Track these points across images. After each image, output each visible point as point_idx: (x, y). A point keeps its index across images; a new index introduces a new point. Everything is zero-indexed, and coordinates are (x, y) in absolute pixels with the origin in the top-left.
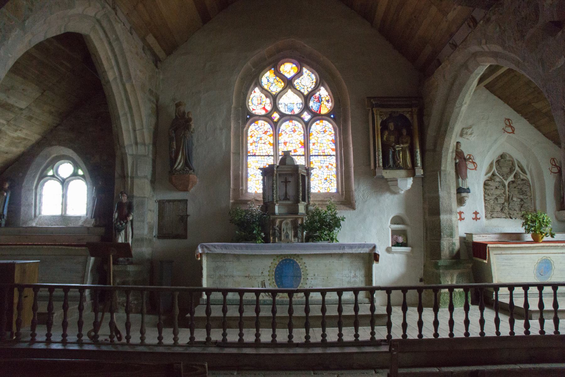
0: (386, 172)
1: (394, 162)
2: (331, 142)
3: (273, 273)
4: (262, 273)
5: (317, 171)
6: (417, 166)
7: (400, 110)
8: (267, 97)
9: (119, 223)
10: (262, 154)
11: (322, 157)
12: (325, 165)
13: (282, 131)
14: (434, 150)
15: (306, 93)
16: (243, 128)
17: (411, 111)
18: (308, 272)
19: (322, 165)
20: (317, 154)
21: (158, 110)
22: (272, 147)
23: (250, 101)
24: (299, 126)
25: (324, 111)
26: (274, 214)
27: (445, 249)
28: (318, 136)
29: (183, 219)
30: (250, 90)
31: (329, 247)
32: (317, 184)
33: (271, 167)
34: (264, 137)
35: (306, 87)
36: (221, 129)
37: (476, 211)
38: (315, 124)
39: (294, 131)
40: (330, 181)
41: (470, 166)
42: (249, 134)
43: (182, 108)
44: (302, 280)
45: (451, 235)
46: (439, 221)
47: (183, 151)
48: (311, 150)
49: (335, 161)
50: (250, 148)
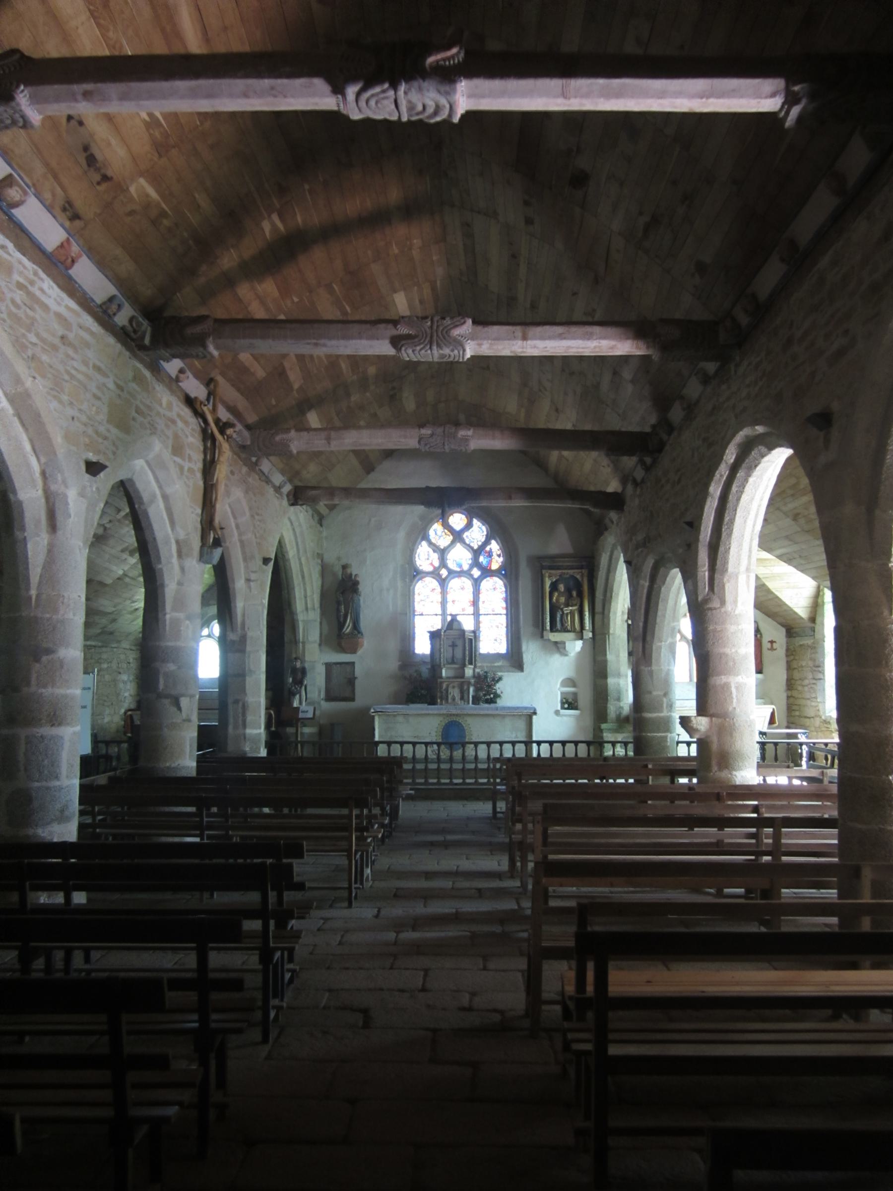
1: (562, 625)
6: (585, 630)
7: (571, 572)
8: (434, 551)
9: (293, 688)
14: (603, 613)
15: (476, 547)
16: (410, 586)
17: (581, 572)
21: (325, 569)
23: (417, 556)
24: (468, 583)
25: (495, 566)
26: (441, 677)
27: (612, 712)
29: (351, 681)
30: (417, 544)
31: (488, 709)
33: (439, 631)
35: (475, 541)
36: (388, 590)
43: (349, 571)
45: (619, 699)
46: (606, 685)
47: (351, 613)
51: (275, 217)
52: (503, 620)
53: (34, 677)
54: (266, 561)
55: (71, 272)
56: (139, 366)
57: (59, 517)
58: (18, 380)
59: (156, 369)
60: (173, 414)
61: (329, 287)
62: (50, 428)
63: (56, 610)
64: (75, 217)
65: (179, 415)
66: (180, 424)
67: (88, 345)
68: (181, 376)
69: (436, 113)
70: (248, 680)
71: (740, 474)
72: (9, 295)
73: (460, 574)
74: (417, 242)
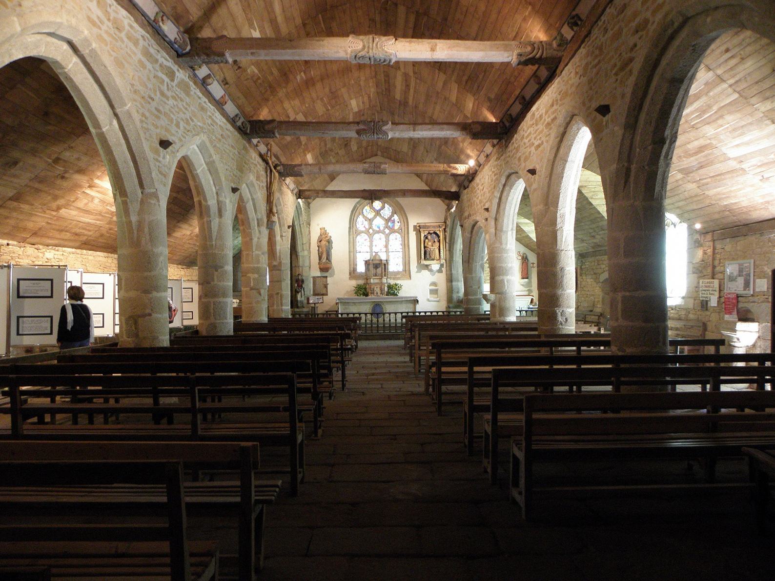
33: (369, 260)
45: (458, 292)
51: (302, 74)
52: (401, 254)
53: (215, 277)
54: (289, 227)
55: (224, 107)
56: (245, 142)
57: (223, 211)
58: (211, 156)
59: (249, 142)
60: (255, 162)
61: (322, 99)
62: (221, 175)
63: (223, 250)
64: (227, 83)
65: (258, 162)
66: (258, 166)
67: (229, 137)
68: (259, 144)
69: (384, 62)
70: (283, 283)
71: (507, 188)
72: (207, 121)
73: (378, 232)
74: (363, 78)
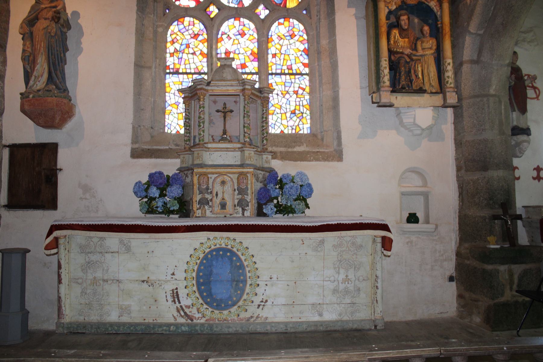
0: (396, 98)
2: (303, 54)
3: (194, 275)
4: (173, 274)
5: (280, 98)
10: (188, 71)
11: (288, 76)
12: (291, 89)
13: (222, 35)
18: (258, 273)
19: (287, 89)
20: (279, 71)
22: (205, 60)
28: (281, 42)
32: (279, 120)
34: (193, 43)
37: (538, 166)
38: (276, 24)
39: (243, 34)
40: (301, 115)
41: (530, 93)
42: (169, 39)
44: (248, 286)
48: (270, 65)
49: (308, 83)
50: (170, 61)
